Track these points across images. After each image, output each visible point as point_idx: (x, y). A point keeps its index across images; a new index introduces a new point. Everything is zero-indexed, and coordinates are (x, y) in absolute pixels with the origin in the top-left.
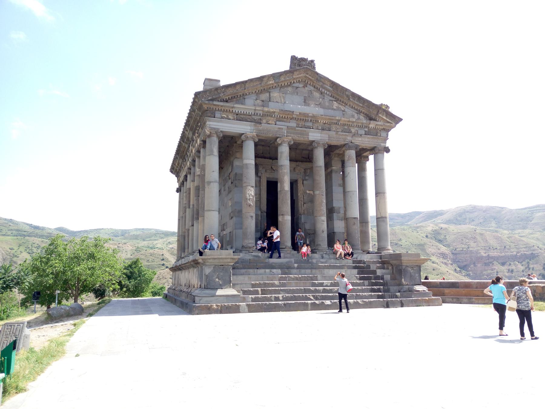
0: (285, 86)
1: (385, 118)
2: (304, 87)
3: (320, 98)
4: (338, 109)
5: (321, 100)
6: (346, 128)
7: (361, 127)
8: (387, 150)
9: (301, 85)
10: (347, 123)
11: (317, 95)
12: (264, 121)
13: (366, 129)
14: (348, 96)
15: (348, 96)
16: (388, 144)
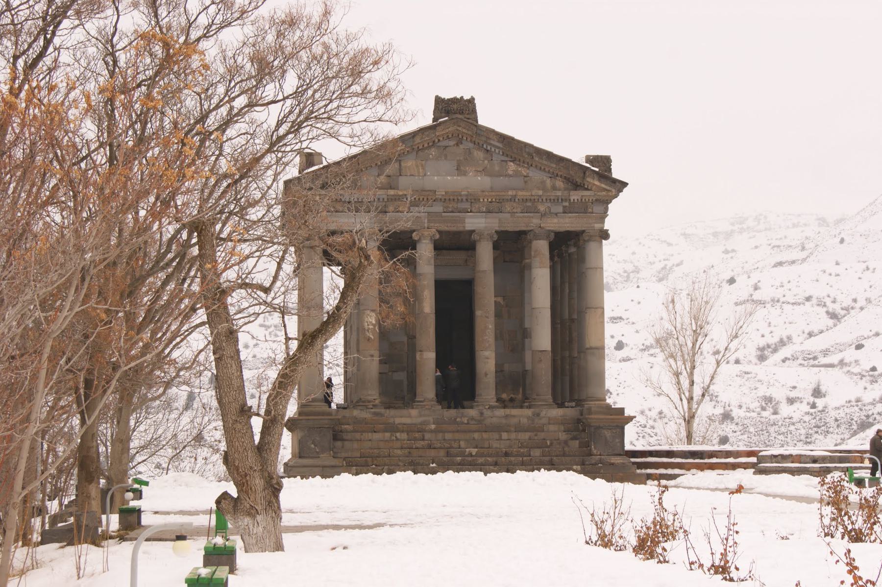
0: (424, 149)
1: (597, 183)
2: (457, 145)
3: (485, 159)
4: (517, 174)
5: (486, 162)
6: (530, 206)
7: (556, 201)
8: (605, 235)
9: (452, 143)
10: (528, 198)
11: (479, 155)
12: (391, 208)
13: (567, 204)
14: (529, 154)
15: (529, 154)
16: (608, 224)
